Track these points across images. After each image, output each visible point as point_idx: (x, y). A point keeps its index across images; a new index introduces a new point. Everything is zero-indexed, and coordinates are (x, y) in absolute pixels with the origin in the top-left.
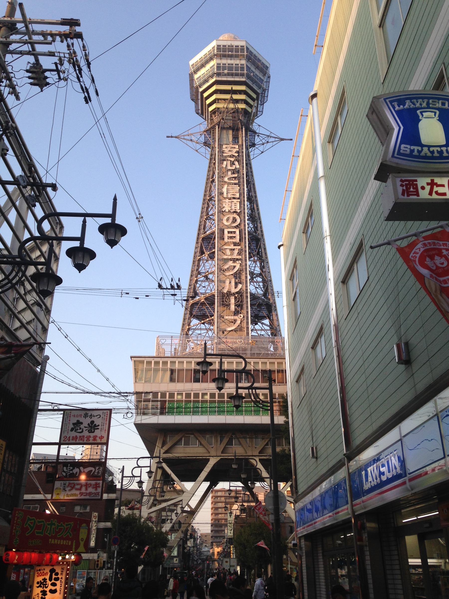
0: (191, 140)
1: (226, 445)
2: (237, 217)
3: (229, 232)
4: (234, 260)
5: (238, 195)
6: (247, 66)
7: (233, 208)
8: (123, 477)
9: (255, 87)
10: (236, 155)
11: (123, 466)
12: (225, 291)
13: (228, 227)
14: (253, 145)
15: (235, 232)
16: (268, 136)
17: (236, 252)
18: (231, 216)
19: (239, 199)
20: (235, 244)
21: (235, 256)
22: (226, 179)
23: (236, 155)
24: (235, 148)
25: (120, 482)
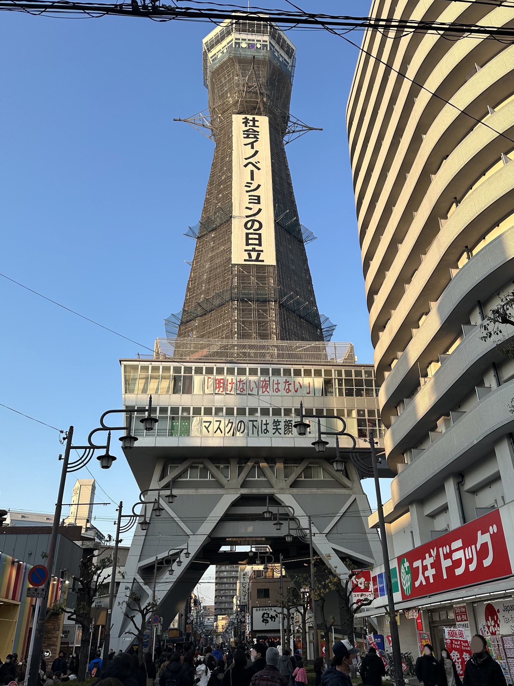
0: (203, 125)
1: (246, 478)
6: (270, 43)
8: (69, 447)
11: (72, 428)
16: (295, 123)
25: (63, 457)
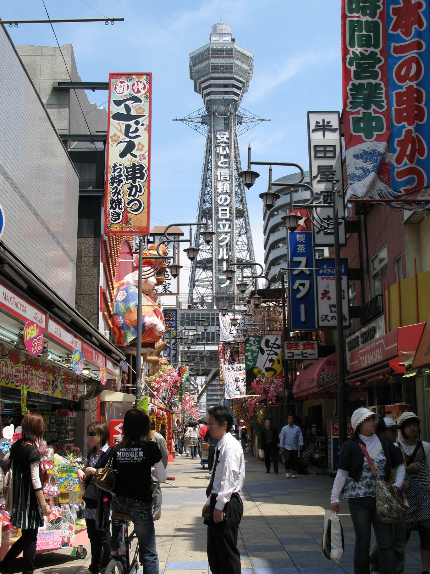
2: (228, 198)
3: (222, 210)
4: (226, 233)
5: (228, 179)
7: (225, 189)
9: (241, 79)
10: (227, 141)
12: (220, 257)
13: (221, 205)
14: (241, 123)
15: (226, 210)
17: (227, 226)
18: (223, 196)
19: (229, 181)
20: (227, 220)
21: (226, 230)
22: (219, 164)
23: (227, 141)
24: (225, 134)
